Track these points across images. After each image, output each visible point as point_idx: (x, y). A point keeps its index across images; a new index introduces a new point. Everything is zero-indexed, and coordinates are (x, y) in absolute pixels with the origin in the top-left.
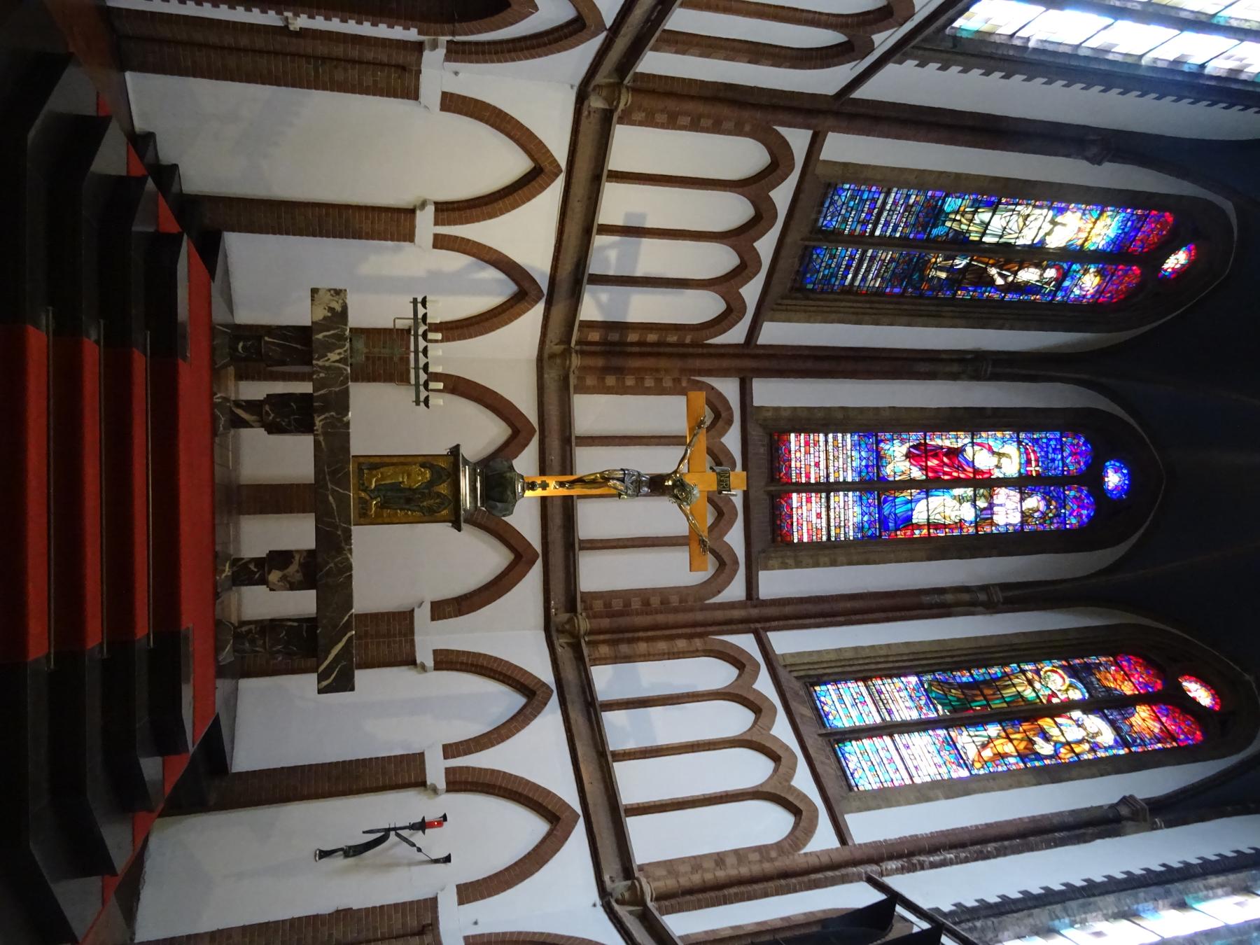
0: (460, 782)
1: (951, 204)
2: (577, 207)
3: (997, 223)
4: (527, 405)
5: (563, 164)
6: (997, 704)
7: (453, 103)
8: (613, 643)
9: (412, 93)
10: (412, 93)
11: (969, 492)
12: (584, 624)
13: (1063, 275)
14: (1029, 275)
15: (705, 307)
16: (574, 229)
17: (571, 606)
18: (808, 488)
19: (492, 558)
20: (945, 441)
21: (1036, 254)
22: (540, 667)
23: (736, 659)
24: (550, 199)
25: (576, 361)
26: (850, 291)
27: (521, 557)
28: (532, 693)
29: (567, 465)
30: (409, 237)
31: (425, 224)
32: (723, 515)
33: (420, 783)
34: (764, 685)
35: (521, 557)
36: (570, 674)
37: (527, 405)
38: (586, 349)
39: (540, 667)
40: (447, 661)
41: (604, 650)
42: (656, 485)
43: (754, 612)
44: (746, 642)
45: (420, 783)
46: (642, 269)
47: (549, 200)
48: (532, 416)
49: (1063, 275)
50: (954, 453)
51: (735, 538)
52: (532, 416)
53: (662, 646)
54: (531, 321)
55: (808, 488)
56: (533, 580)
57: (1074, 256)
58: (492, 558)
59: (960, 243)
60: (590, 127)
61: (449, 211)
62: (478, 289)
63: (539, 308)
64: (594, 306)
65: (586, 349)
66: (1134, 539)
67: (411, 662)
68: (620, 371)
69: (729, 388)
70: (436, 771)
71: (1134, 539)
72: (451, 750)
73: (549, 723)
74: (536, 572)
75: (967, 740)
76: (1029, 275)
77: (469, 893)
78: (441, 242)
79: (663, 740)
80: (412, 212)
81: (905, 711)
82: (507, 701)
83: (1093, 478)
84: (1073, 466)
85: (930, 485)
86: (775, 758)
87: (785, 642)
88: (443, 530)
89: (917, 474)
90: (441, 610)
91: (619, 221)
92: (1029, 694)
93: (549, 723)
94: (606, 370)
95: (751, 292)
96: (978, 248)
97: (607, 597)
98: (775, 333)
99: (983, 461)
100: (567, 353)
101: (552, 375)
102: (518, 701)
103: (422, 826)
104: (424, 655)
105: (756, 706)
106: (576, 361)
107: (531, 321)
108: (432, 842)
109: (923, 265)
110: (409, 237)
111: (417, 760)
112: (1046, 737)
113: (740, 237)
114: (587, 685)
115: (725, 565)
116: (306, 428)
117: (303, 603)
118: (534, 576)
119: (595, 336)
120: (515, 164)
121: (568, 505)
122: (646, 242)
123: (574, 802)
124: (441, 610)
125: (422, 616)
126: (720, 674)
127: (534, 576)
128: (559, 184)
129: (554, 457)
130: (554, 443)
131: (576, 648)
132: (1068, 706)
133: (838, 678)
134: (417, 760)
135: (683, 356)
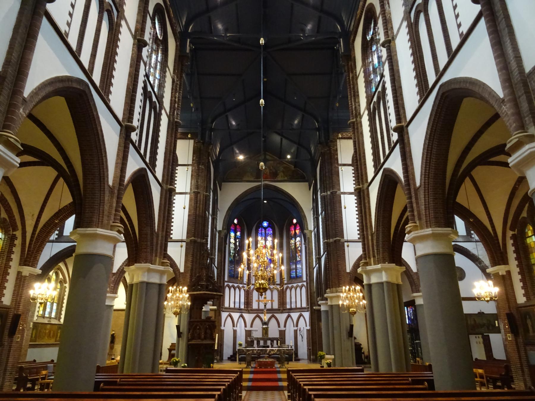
0: (297, 326)
1: (230, 259)
2: (233, 310)
3: (232, 252)
4: (254, 315)
5: (228, 313)
6: (294, 252)
7: (224, 326)
8: (284, 304)
9: (224, 330)
10: (224, 330)
12: (281, 309)
13: (238, 238)
14: (238, 244)
16: (235, 311)
17: (280, 310)
19: (273, 320)
21: (235, 244)
22: (286, 315)
23: (287, 288)
24: (232, 314)
25: (249, 309)
27: (273, 316)
28: (289, 316)
29: (262, 310)
30: (236, 330)
31: (235, 328)
33: (297, 330)
34: (290, 286)
35: (273, 316)
36: (287, 311)
37: (254, 315)
38: (247, 307)
39: (287, 314)
40: (285, 326)
41: (285, 306)
42: (265, 306)
44: (285, 286)
45: (297, 330)
46: (238, 301)
47: (232, 314)
48: (256, 314)
49: (238, 238)
52: (256, 314)
54: (245, 315)
56: (276, 315)
57: (235, 238)
58: (273, 320)
59: (234, 256)
60: (226, 310)
61: (234, 326)
62: (241, 321)
63: (243, 314)
64: (242, 307)
65: (247, 307)
66: (275, 224)
68: (250, 302)
70: (296, 328)
71: (275, 224)
72: (294, 327)
73: (292, 314)
75: (298, 259)
76: (238, 244)
77: (306, 326)
78: (237, 327)
79: (295, 301)
80: (234, 330)
82: (289, 319)
83: (265, 228)
84: (263, 231)
86: (297, 287)
88: (269, 329)
90: (279, 326)
91: (233, 305)
92: (293, 247)
93: (292, 314)
94: (250, 304)
95: (241, 286)
96: (235, 254)
97: (279, 305)
100: (248, 310)
101: (251, 312)
102: (290, 318)
103: (300, 330)
104: (284, 329)
105: (292, 287)
106: (249, 309)
107: (245, 315)
108: (302, 329)
109: (237, 260)
110: (236, 330)
111: (295, 330)
112: (298, 247)
113: (235, 289)
114: (289, 309)
116: (259, 341)
117: (275, 342)
118: (275, 314)
119: (246, 306)
120: (229, 318)
121: (268, 310)
122: (236, 301)
123: (300, 313)
124: (279, 326)
125: (280, 329)
126: (288, 291)
127: (275, 314)
128: (231, 313)
129: (261, 312)
130: (259, 311)
131: (284, 310)
132: (295, 241)
133: (291, 274)
134: (295, 330)
135: (248, 294)
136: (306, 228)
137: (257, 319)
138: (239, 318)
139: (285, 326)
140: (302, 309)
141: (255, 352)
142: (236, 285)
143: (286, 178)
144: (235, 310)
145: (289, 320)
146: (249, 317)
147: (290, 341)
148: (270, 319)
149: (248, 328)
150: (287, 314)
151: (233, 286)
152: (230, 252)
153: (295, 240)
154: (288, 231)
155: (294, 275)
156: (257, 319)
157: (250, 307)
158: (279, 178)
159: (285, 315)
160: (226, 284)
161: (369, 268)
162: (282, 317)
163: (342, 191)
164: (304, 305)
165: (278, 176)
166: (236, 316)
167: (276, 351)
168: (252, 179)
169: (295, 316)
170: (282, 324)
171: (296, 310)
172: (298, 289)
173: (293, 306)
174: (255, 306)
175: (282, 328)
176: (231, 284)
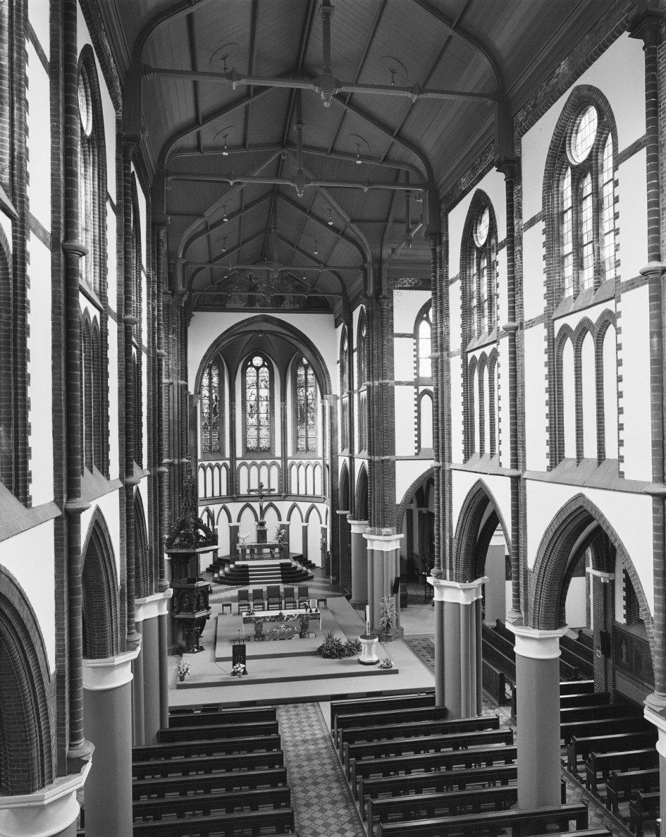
0: (307, 521)
3: (206, 411)
5: (205, 507)
11: (260, 402)
12: (284, 494)
15: (224, 470)
17: (281, 496)
18: (258, 443)
19: (271, 511)
20: (249, 409)
21: (210, 398)
25: (234, 496)
26: (219, 439)
27: (271, 505)
32: (264, 464)
35: (271, 505)
36: (293, 498)
39: (291, 503)
40: (289, 519)
43: (283, 460)
50: (251, 407)
51: (268, 462)
53: (289, 479)
54: (229, 506)
55: (258, 443)
56: (275, 503)
58: (271, 511)
67: (289, 525)
69: (238, 462)
70: (305, 524)
74: (274, 503)
81: (304, 433)
85: (258, 412)
87: (290, 454)
89: (256, 416)
90: (280, 520)
98: (228, 455)
99: (253, 398)
104: (287, 523)
107: (229, 506)
111: (303, 526)
115: (274, 464)
130: (250, 499)
134: (303, 526)
136: (328, 392)
137: (248, 511)
138: (221, 509)
139: (289, 519)
140: (312, 498)
141: (268, 620)
142: (213, 463)
143: (297, 306)
144: (214, 500)
145: (296, 511)
146: (235, 508)
147: (296, 548)
148: (267, 508)
149: (234, 523)
150: (291, 503)
151: (210, 466)
152: (202, 412)
153: (307, 391)
154: (295, 376)
155: (302, 444)
156: (248, 511)
157: (236, 493)
158: (286, 305)
159: (288, 504)
160: (199, 463)
161: (443, 582)
162: (284, 506)
163: (397, 379)
164: (319, 492)
165: (285, 302)
166: (215, 508)
167: (296, 618)
168: (242, 306)
169: (304, 506)
170: (284, 517)
171: (305, 498)
172: (310, 469)
173: (302, 492)
174: (243, 490)
175: (284, 521)
176: (206, 463)
